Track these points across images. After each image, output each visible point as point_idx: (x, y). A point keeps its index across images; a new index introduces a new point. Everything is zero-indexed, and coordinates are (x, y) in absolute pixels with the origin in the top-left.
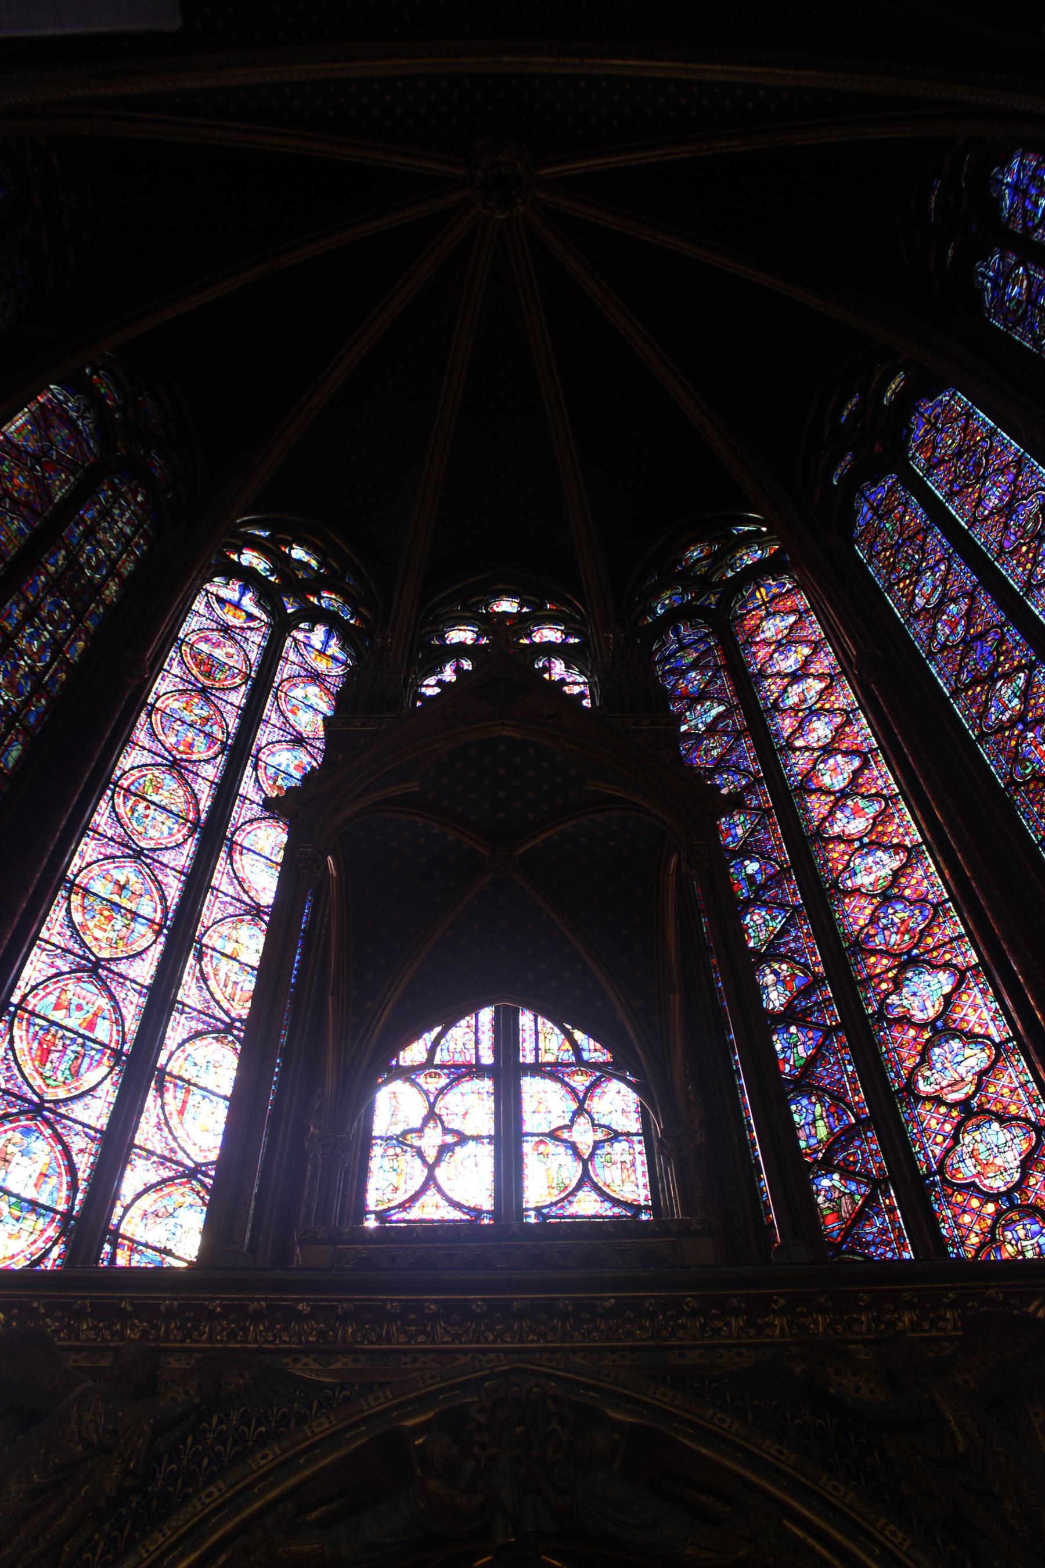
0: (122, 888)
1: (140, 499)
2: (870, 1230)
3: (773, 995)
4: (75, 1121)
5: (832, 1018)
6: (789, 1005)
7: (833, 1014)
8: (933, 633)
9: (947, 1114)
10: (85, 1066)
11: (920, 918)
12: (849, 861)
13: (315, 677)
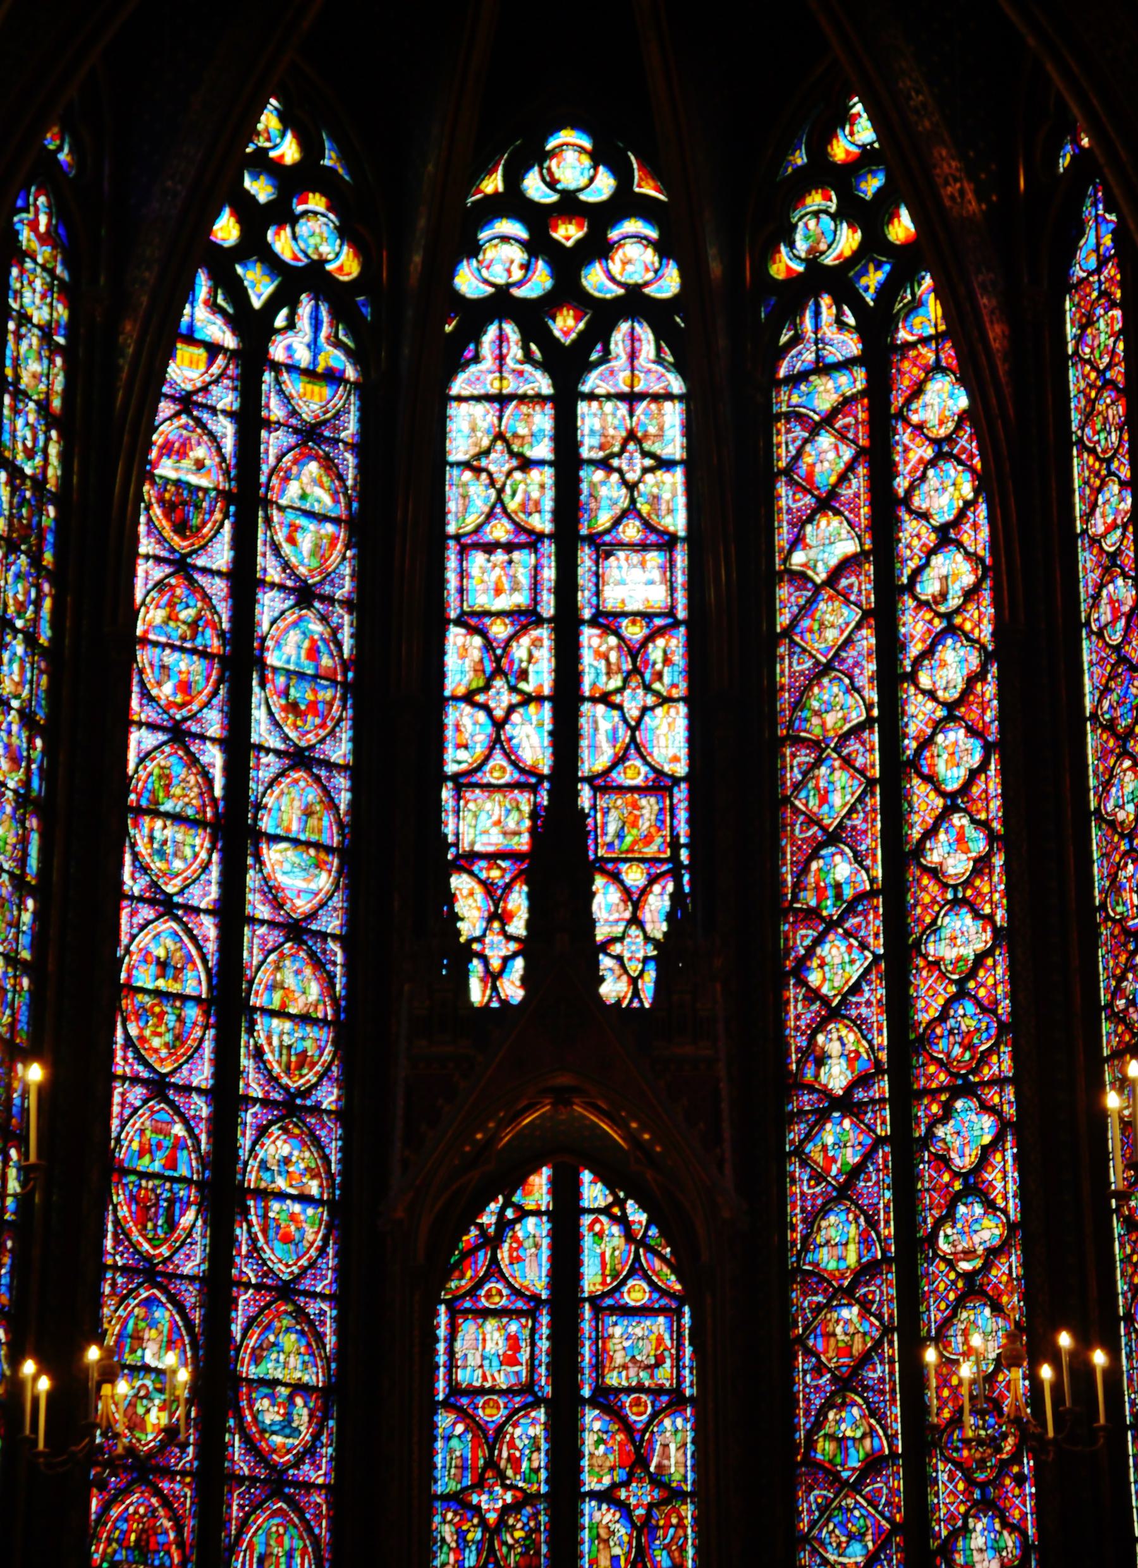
0: (163, 966)
1: (43, 220)
3: (835, 1070)
4: (182, 1277)
6: (850, 1089)
7: (884, 1122)
8: (1097, 597)
9: (954, 1282)
10: (177, 1212)
11: (985, 1035)
12: (938, 913)
13: (311, 436)
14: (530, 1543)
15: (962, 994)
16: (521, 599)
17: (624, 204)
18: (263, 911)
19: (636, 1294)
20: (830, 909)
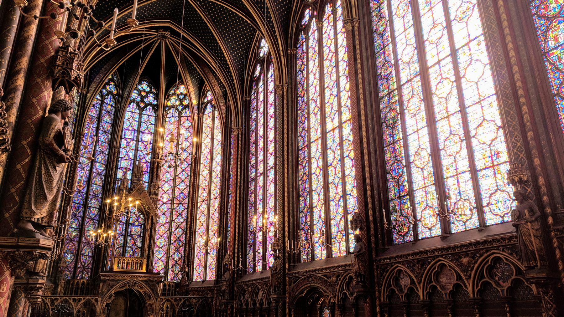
2: (165, 235)
5: (170, 206)
14: (119, 253)
15: (182, 193)
16: (132, 137)
17: (150, 92)
18: (95, 171)
19: (137, 223)
20: (166, 180)
